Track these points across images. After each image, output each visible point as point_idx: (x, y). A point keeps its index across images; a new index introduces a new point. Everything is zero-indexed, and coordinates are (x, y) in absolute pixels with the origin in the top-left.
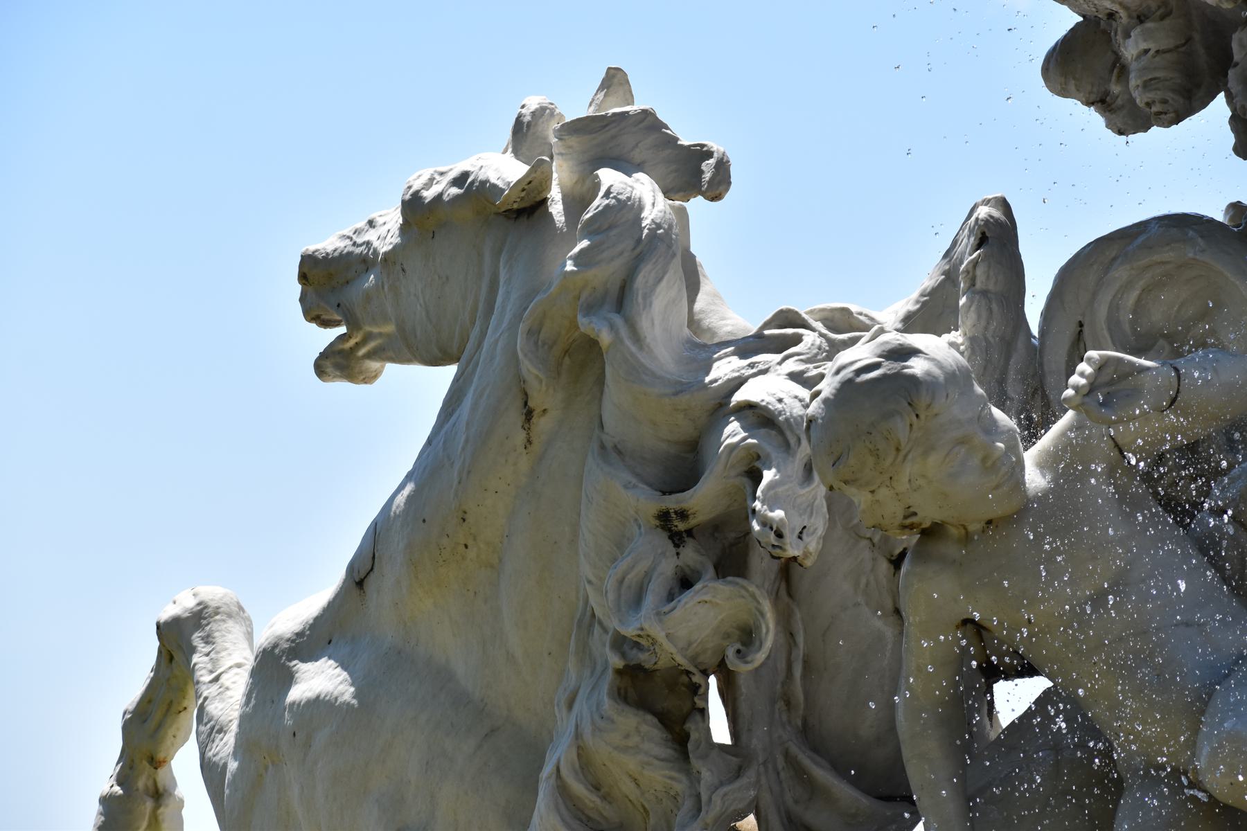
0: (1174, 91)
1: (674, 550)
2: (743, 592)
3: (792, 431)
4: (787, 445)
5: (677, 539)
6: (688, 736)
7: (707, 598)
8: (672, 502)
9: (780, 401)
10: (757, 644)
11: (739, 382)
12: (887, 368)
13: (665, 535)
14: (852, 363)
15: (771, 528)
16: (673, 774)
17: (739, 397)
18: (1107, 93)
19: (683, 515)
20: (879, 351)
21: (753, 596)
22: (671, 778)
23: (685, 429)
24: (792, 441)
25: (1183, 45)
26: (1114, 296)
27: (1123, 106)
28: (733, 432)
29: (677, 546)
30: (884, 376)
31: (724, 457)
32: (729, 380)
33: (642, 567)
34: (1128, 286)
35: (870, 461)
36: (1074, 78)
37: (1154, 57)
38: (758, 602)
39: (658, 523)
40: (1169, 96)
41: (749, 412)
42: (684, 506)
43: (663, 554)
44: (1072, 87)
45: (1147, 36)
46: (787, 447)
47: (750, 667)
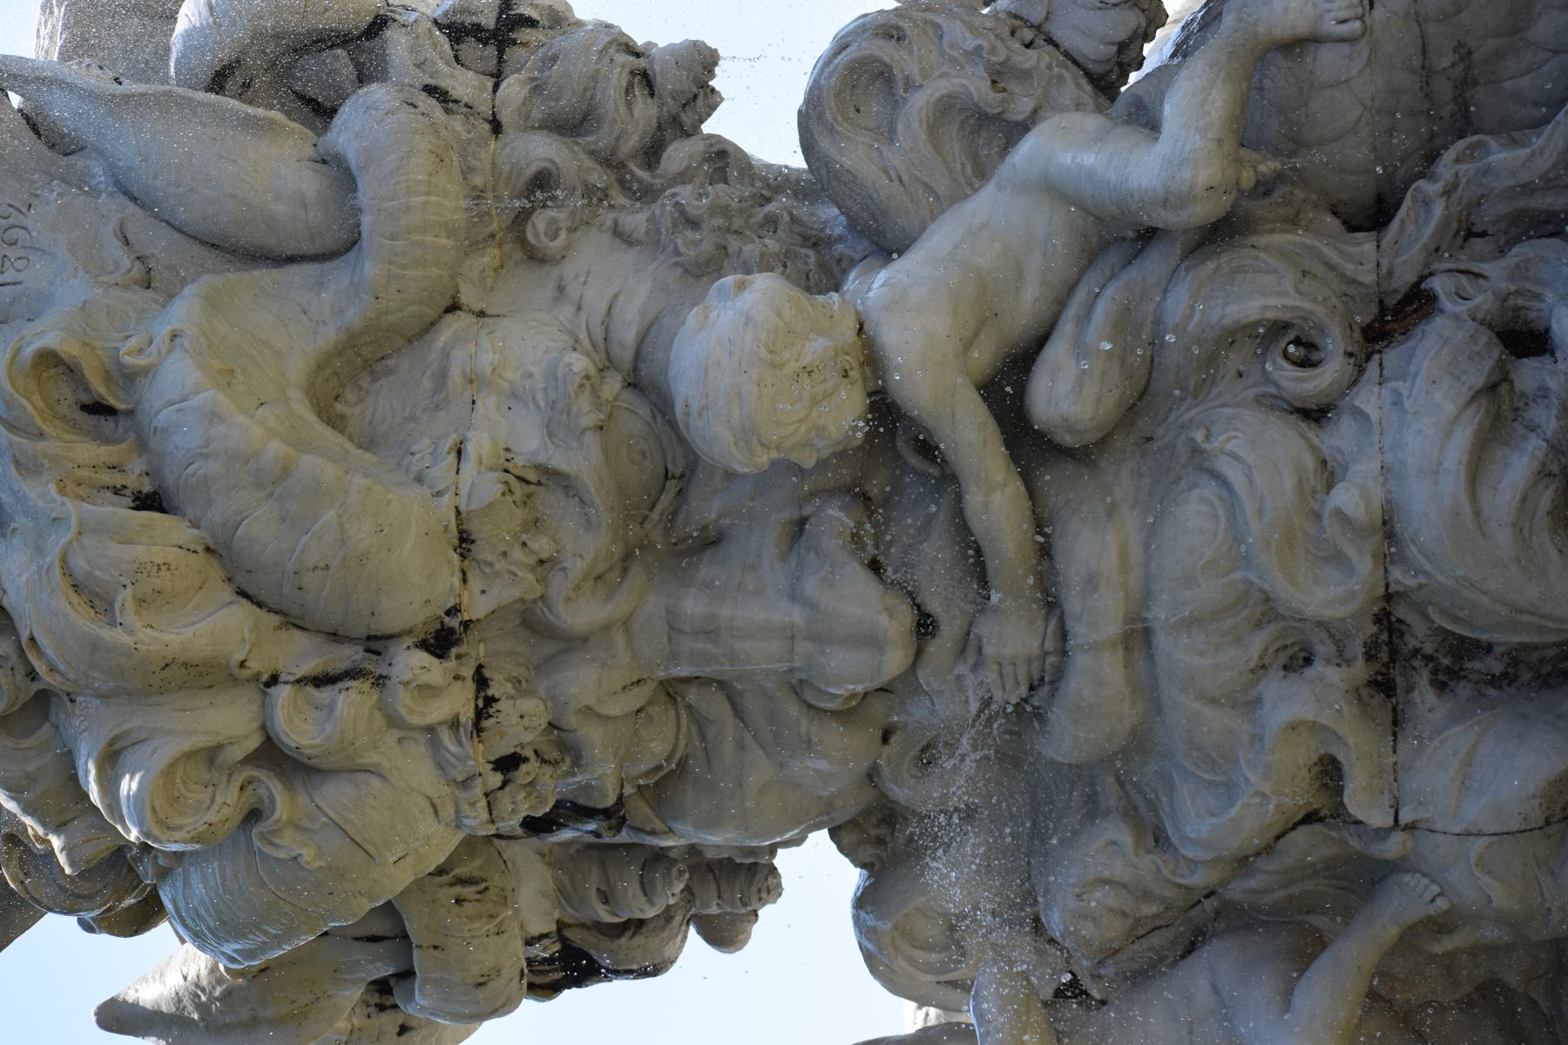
0: (751, 884)
25: (714, 873)
26: (918, 969)
34: (910, 960)
36: (737, 936)
37: (723, 900)
40: (755, 888)
44: (741, 937)
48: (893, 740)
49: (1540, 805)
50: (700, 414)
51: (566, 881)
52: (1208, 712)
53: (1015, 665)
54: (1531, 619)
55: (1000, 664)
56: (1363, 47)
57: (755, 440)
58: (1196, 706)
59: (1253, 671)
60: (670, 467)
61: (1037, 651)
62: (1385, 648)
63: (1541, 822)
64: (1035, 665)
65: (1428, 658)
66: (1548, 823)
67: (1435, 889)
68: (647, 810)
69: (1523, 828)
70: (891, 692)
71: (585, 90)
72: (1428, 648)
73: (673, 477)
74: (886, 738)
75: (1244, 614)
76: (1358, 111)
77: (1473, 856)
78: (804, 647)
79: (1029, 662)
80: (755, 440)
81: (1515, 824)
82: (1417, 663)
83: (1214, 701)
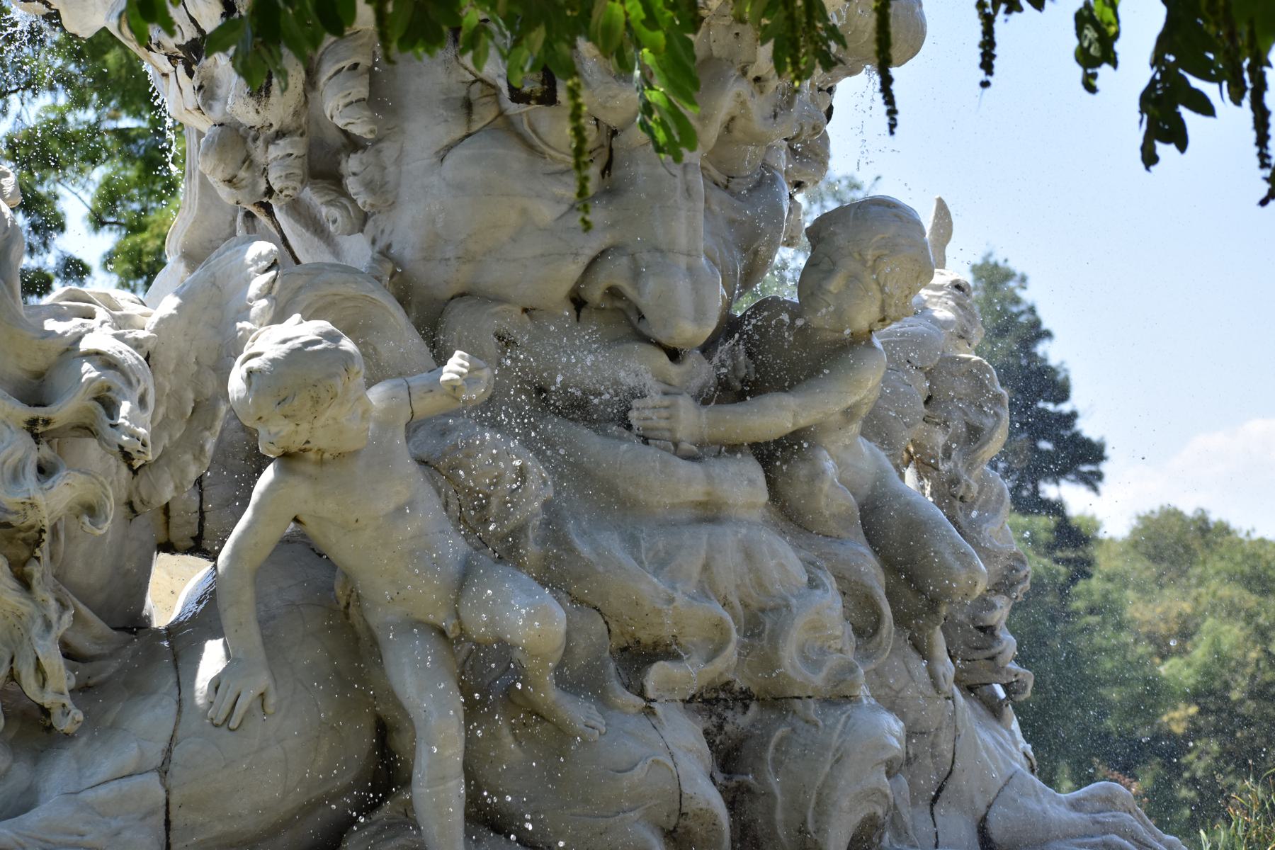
1: (35, 446)
2: (94, 480)
3: (134, 374)
4: (130, 383)
5: (36, 437)
6: (31, 576)
7: (70, 481)
8: (40, 413)
9: (121, 352)
10: (103, 517)
11: (80, 337)
12: (325, 344)
13: (29, 435)
14: (298, 337)
15: (138, 439)
16: (23, 600)
17: (84, 346)
18: (235, 176)
19: (47, 422)
20: (317, 332)
21: (102, 485)
22: (21, 603)
23: (39, 363)
24: (134, 381)
27: (246, 186)
28: (89, 371)
29: (37, 443)
30: (325, 350)
31: (85, 387)
32: (75, 333)
33: (18, 455)
35: (309, 404)
38: (105, 489)
39: (26, 426)
41: (97, 358)
42: (51, 416)
43: (31, 447)
45: (293, 145)
46: (130, 383)
47: (99, 532)
48: (525, 316)
49: (701, 809)
50: (896, 216)
51: (365, 40)
52: (700, 562)
53: (667, 419)
54: (812, 804)
55: (667, 407)
56: (930, 692)
57: (887, 252)
58: (703, 554)
59: (725, 597)
60: (736, 180)
61: (679, 436)
62: (715, 695)
63: (684, 810)
64: (667, 434)
65: (720, 727)
66: (682, 814)
67: (604, 730)
68: (489, 119)
69: (684, 796)
70: (578, 320)
71: (817, 155)
72: (728, 728)
73: (728, 181)
74: (525, 310)
75: (753, 592)
76: (896, 687)
77: (660, 758)
78: (683, 261)
79: (670, 430)
80: (887, 252)
81: (687, 789)
82: (714, 719)
83: (706, 568)
